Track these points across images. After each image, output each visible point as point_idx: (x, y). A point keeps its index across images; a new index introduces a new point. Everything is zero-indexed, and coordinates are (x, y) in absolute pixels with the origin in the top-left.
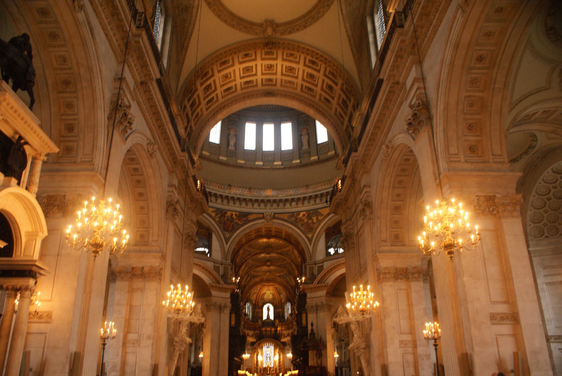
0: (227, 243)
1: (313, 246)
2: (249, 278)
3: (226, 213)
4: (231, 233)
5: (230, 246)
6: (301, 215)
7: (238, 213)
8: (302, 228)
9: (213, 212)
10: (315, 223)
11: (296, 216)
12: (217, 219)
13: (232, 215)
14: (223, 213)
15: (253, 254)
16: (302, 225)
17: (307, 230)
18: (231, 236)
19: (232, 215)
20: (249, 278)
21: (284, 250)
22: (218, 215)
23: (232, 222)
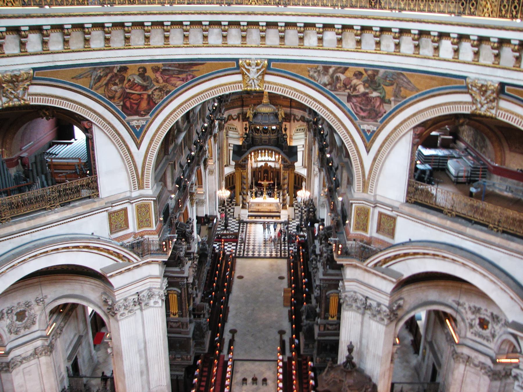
1: (375, 159)
4: (148, 117)
6: (349, 74)
8: (349, 106)
10: (389, 102)
11: (335, 72)
14: (115, 71)
16: (349, 98)
17: (362, 114)
23: (145, 88)
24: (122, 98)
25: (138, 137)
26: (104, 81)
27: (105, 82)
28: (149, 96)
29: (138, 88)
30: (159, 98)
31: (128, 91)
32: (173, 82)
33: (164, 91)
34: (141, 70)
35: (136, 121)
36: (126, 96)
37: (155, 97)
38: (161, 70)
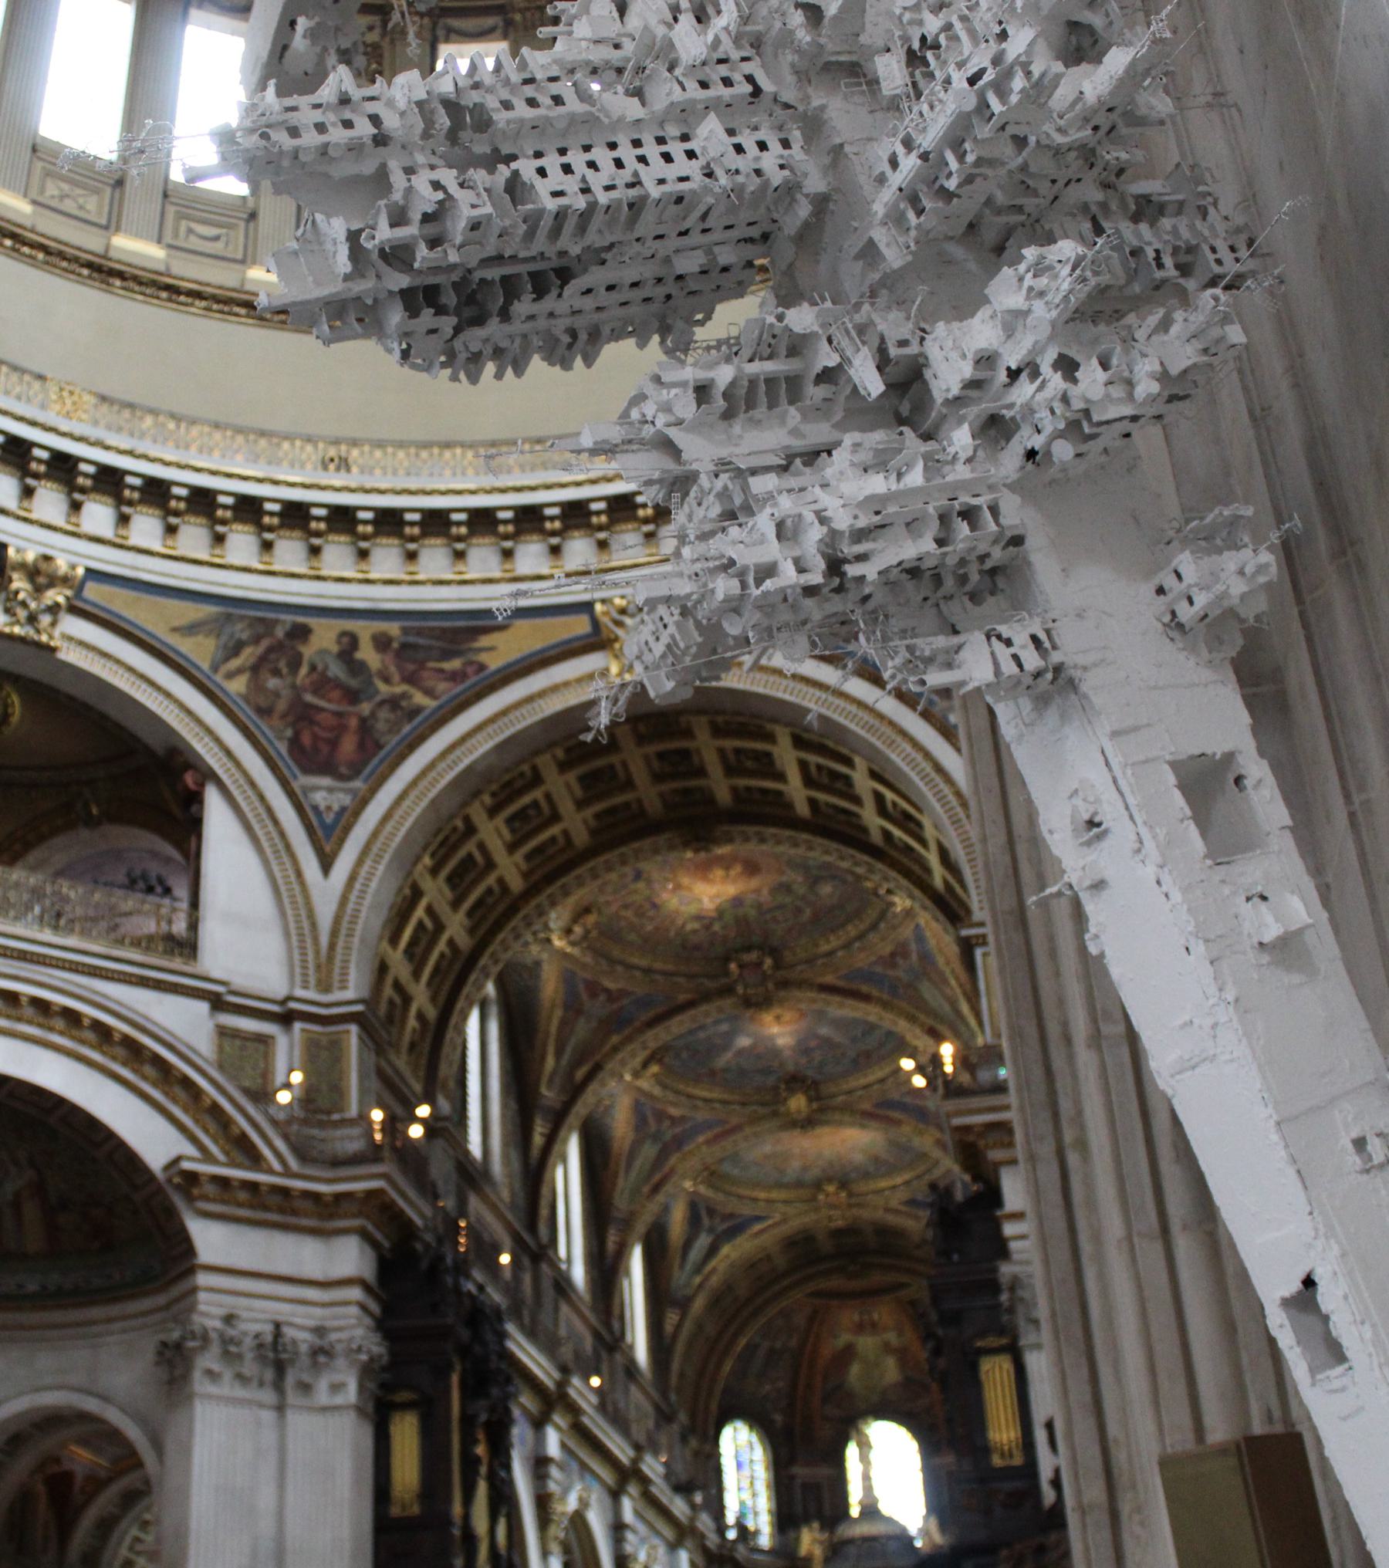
0: (326, 864)
2: (703, 1241)
3: (301, 633)
4: (358, 784)
5: (352, 879)
7: (393, 628)
9: (190, 629)
12: (237, 686)
13: (351, 642)
14: (280, 632)
15: (646, 1016)
18: (362, 802)
19: (351, 642)
20: (703, 1241)
21: (862, 960)
22: (236, 649)
23: (353, 697)
24: (290, 719)
25: (328, 837)
26: (248, 655)
27: (252, 660)
28: (363, 721)
29: (336, 694)
30: (390, 731)
31: (309, 698)
32: (430, 683)
33: (401, 708)
34: (345, 640)
35: (326, 793)
36: (301, 715)
37: (381, 726)
38: (395, 645)
